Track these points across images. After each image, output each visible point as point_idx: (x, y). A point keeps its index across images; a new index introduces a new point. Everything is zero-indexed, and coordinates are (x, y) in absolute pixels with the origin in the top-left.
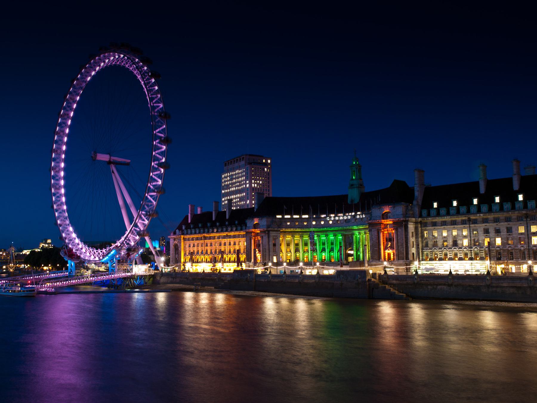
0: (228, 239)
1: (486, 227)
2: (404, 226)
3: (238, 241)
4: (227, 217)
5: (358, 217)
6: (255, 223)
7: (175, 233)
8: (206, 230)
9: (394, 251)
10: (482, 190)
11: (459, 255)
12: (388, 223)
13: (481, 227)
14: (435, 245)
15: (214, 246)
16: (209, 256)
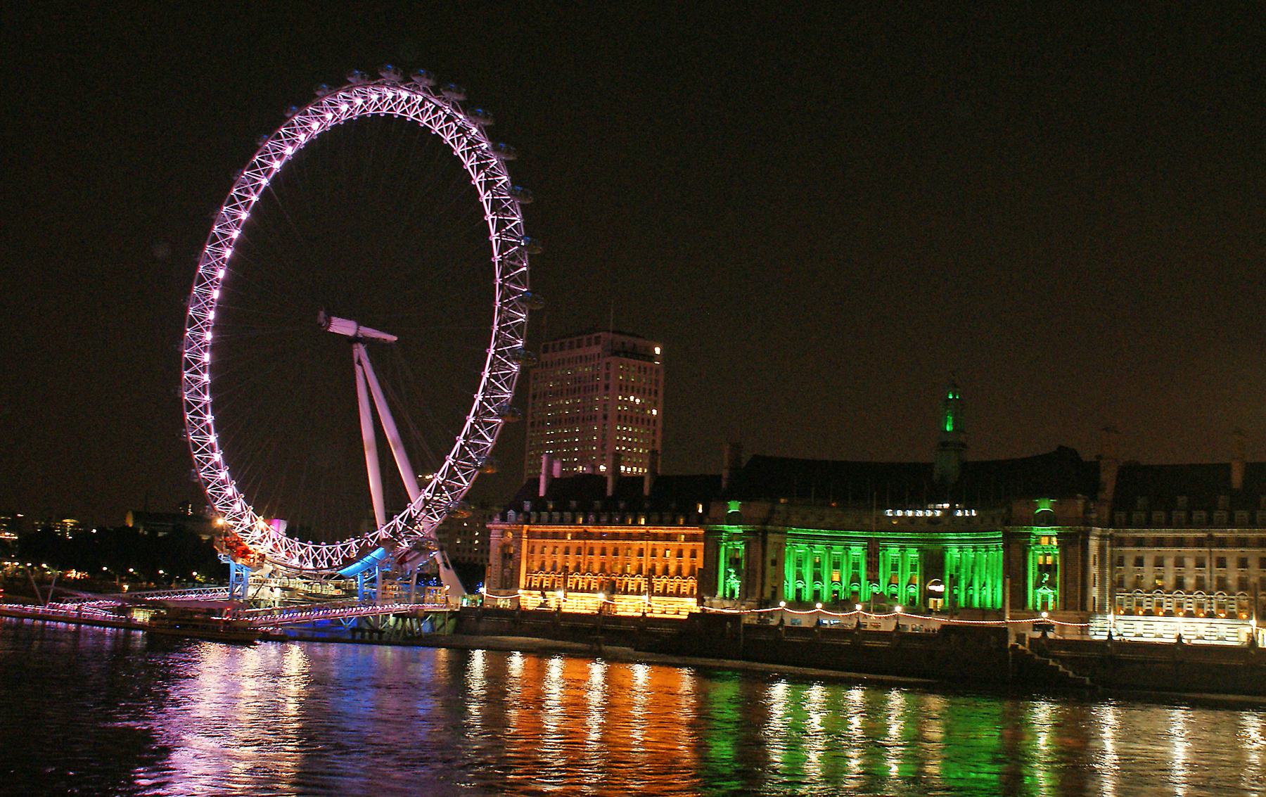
0: (651, 543)
1: (1243, 555)
2: (1080, 542)
3: (677, 548)
4: (646, 492)
5: (959, 513)
6: (729, 512)
7: (504, 519)
8: (592, 518)
9: (1057, 592)
10: (1237, 479)
11: (1186, 605)
12: (1044, 533)
13: (1232, 554)
14: (1137, 585)
15: (611, 555)
16: (596, 577)
